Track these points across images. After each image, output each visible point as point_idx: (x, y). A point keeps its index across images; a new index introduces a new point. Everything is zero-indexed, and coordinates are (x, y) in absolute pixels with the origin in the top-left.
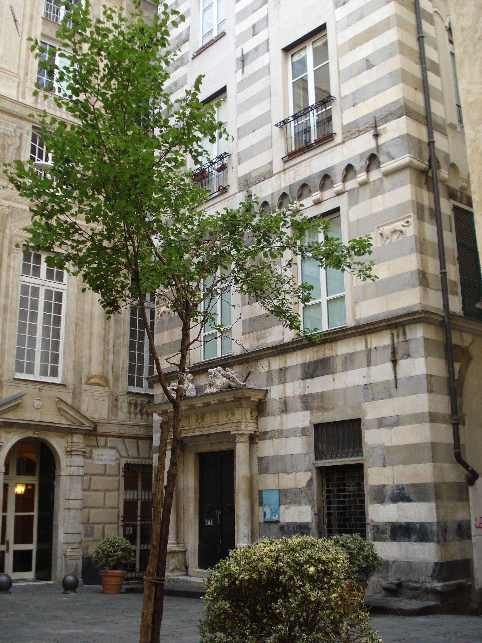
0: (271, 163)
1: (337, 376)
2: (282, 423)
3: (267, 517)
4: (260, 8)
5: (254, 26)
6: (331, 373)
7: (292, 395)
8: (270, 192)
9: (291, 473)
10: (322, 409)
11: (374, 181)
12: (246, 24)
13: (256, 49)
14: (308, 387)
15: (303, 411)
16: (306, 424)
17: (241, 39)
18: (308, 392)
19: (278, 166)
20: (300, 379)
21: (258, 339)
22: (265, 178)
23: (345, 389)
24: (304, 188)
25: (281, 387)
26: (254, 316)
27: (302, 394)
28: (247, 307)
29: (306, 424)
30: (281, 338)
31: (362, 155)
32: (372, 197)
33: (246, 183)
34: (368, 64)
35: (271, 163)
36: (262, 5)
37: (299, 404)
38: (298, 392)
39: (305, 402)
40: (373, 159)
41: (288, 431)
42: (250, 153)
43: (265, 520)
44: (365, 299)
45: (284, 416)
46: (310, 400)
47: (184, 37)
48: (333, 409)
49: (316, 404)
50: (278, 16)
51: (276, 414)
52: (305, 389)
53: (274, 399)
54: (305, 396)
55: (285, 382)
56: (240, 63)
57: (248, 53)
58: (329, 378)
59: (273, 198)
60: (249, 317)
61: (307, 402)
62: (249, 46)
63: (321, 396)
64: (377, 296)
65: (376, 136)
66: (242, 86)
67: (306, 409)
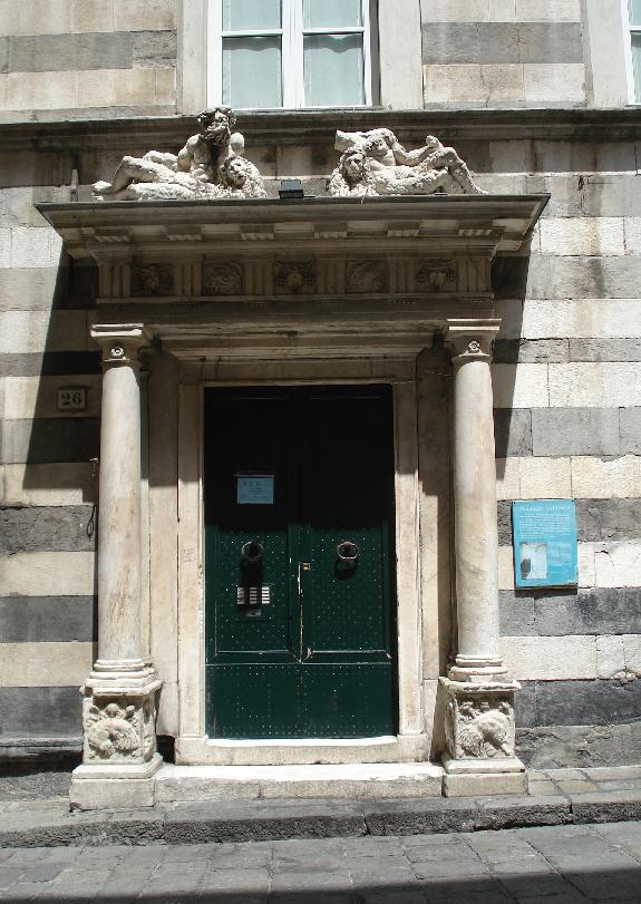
3: (531, 575)
9: (619, 456)
25: (580, 224)
26: (472, 18)
41: (602, 344)
43: (522, 584)
45: (592, 303)
51: (559, 293)
55: (594, 214)
60: (452, 20)
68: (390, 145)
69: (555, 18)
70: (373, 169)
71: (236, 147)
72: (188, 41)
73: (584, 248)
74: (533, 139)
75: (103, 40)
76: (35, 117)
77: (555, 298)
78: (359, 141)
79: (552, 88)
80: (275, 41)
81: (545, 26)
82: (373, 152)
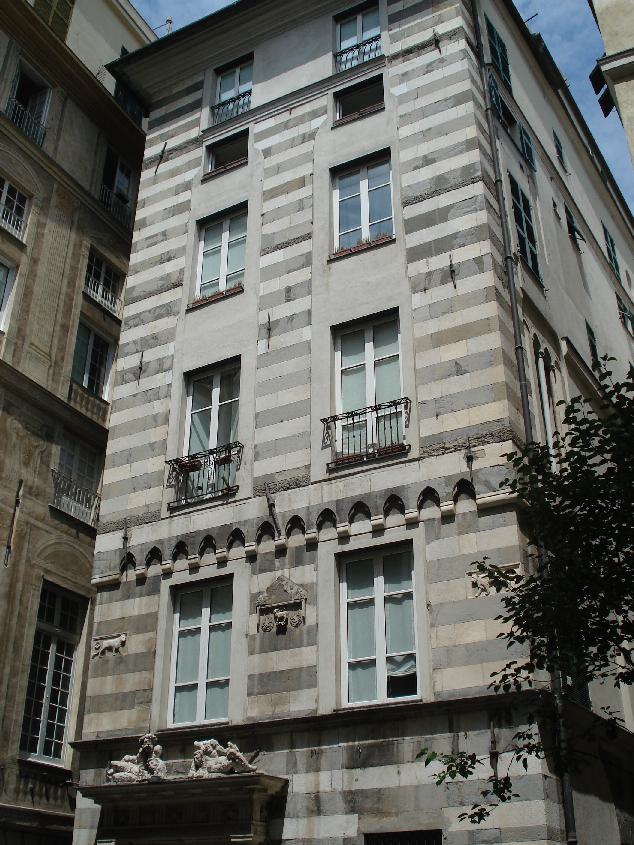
0: (308, 467)
1: (405, 768)
2: (310, 830)
4: (299, 269)
5: (289, 290)
6: (396, 763)
7: (328, 789)
8: (305, 505)
10: (378, 813)
11: (464, 514)
12: (278, 284)
13: (291, 318)
14: (357, 780)
15: (346, 813)
16: (352, 832)
17: (265, 302)
18: (356, 787)
19: (319, 472)
20: (343, 767)
21: (275, 705)
22: (298, 485)
23: (418, 786)
24: (360, 509)
25: (311, 776)
27: (346, 789)
28: (256, 658)
29: (352, 832)
30: (313, 707)
31: (448, 479)
32: (460, 533)
33: (266, 488)
34: (458, 369)
35: (308, 467)
36: (303, 266)
37: (340, 804)
38: (339, 787)
39: (349, 802)
40: (465, 488)
42: (275, 448)
44: (449, 665)
45: (316, 819)
46: (359, 799)
47: (174, 280)
48: (397, 814)
49: (368, 805)
50: (327, 285)
51: (300, 814)
52: (350, 783)
53: (298, 794)
54: (350, 792)
55: (318, 770)
56: (264, 332)
57: (278, 321)
58: (391, 769)
59: (308, 514)
61: (354, 802)
62: (281, 311)
63: (379, 794)
64: (467, 663)
65: (470, 459)
66: (264, 360)
67: (353, 811)
68: (214, 748)
69: (305, 665)
70: (207, 760)
71: (156, 753)
72: (156, 694)
73: (312, 789)
74: (292, 732)
75: (125, 695)
76: (98, 736)
77: (298, 817)
78: (202, 744)
79: (300, 704)
80: (195, 686)
81: (301, 669)
82: (207, 753)
